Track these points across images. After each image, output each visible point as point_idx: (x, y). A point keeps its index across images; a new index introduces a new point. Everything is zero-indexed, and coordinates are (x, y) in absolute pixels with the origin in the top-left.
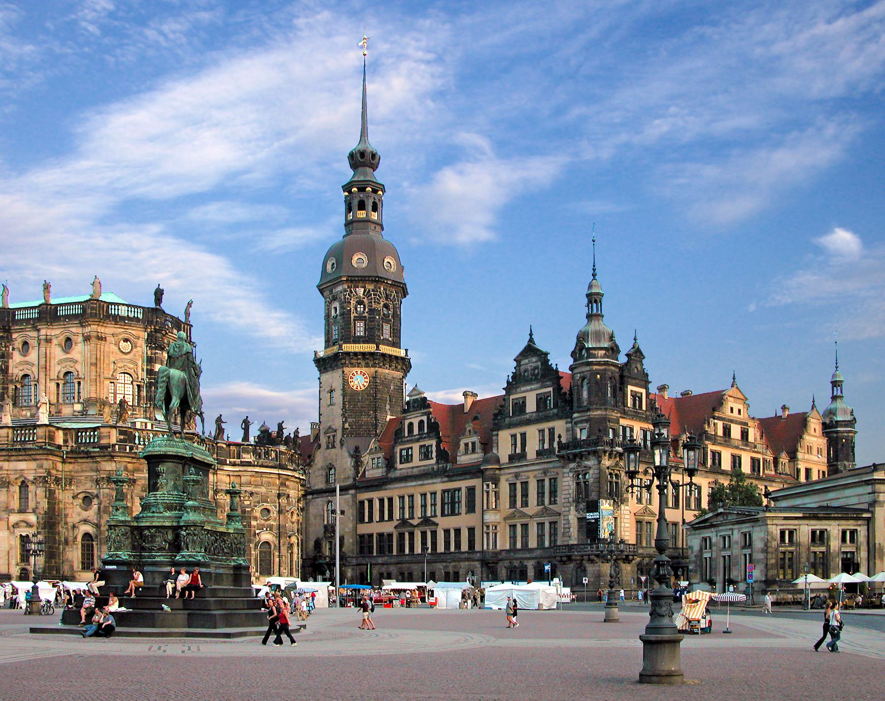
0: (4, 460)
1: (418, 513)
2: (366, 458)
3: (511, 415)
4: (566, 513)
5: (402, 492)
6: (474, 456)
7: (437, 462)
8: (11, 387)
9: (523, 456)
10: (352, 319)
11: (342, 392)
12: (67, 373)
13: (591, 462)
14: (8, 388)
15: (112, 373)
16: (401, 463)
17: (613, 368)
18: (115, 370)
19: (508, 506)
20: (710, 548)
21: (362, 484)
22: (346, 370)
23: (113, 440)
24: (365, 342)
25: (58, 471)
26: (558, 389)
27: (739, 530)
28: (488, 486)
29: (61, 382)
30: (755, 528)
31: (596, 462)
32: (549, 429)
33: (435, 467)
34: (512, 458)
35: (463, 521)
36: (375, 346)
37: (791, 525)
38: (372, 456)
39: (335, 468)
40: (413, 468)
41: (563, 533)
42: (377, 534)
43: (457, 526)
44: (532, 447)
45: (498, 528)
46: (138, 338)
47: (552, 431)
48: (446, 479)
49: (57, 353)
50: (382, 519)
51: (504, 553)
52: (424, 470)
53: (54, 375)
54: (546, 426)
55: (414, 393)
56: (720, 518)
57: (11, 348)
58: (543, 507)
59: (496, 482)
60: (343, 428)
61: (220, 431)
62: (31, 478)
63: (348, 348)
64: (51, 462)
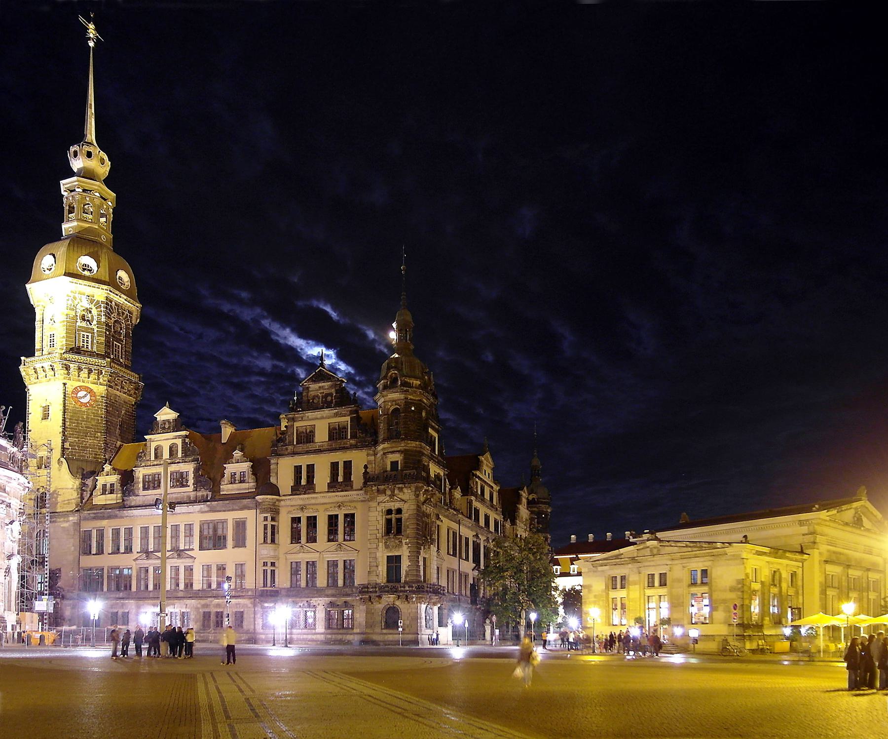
3: (295, 443)
4: (373, 551)
7: (195, 490)
9: (310, 486)
16: (144, 489)
19: (289, 541)
33: (192, 495)
34: (297, 489)
43: (220, 561)
44: (322, 478)
50: (116, 551)
52: (176, 498)
54: (340, 457)
59: (275, 512)
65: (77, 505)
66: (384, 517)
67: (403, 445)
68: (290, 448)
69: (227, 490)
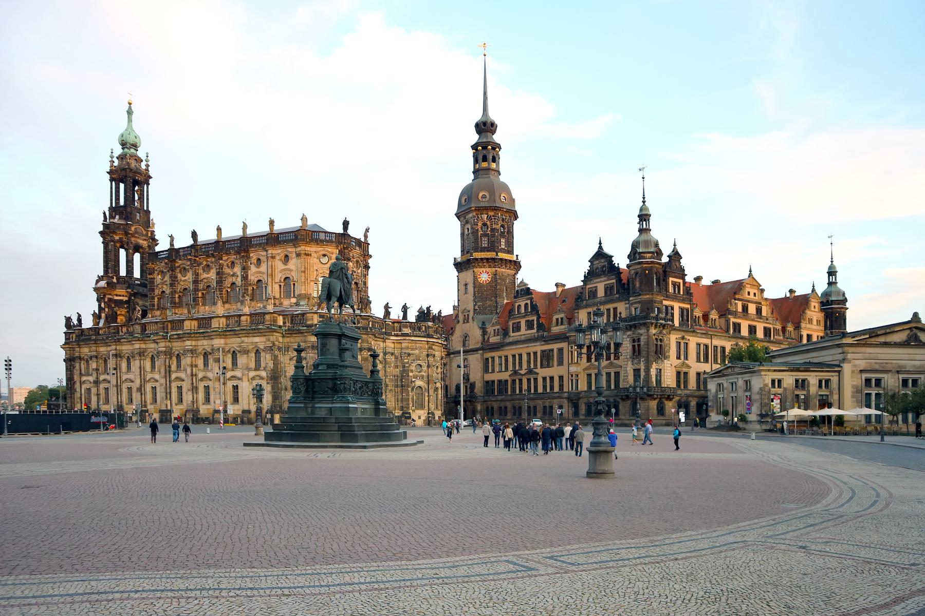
0: (245, 336)
1: (525, 366)
2: (490, 330)
4: (625, 366)
5: (516, 352)
6: (563, 327)
7: (538, 331)
8: (250, 288)
10: (479, 235)
12: (286, 278)
13: (642, 331)
14: (247, 289)
15: (315, 277)
17: (657, 266)
18: (317, 275)
20: (723, 391)
21: (487, 347)
22: (475, 269)
23: (315, 322)
24: (488, 251)
25: (279, 342)
26: (619, 280)
27: (742, 378)
28: (572, 347)
29: (282, 284)
30: (754, 378)
31: (646, 331)
33: (536, 335)
35: (555, 371)
37: (777, 376)
38: (494, 328)
40: (521, 335)
41: (624, 379)
43: (551, 375)
45: (579, 376)
46: (333, 254)
47: (615, 309)
48: (543, 343)
49: (279, 265)
51: (583, 393)
53: (277, 280)
54: (611, 306)
55: (522, 285)
56: (729, 370)
60: (475, 310)
61: (387, 313)
62: (262, 347)
64: (275, 337)
65: (482, 344)
68: (585, 302)
69: (555, 330)
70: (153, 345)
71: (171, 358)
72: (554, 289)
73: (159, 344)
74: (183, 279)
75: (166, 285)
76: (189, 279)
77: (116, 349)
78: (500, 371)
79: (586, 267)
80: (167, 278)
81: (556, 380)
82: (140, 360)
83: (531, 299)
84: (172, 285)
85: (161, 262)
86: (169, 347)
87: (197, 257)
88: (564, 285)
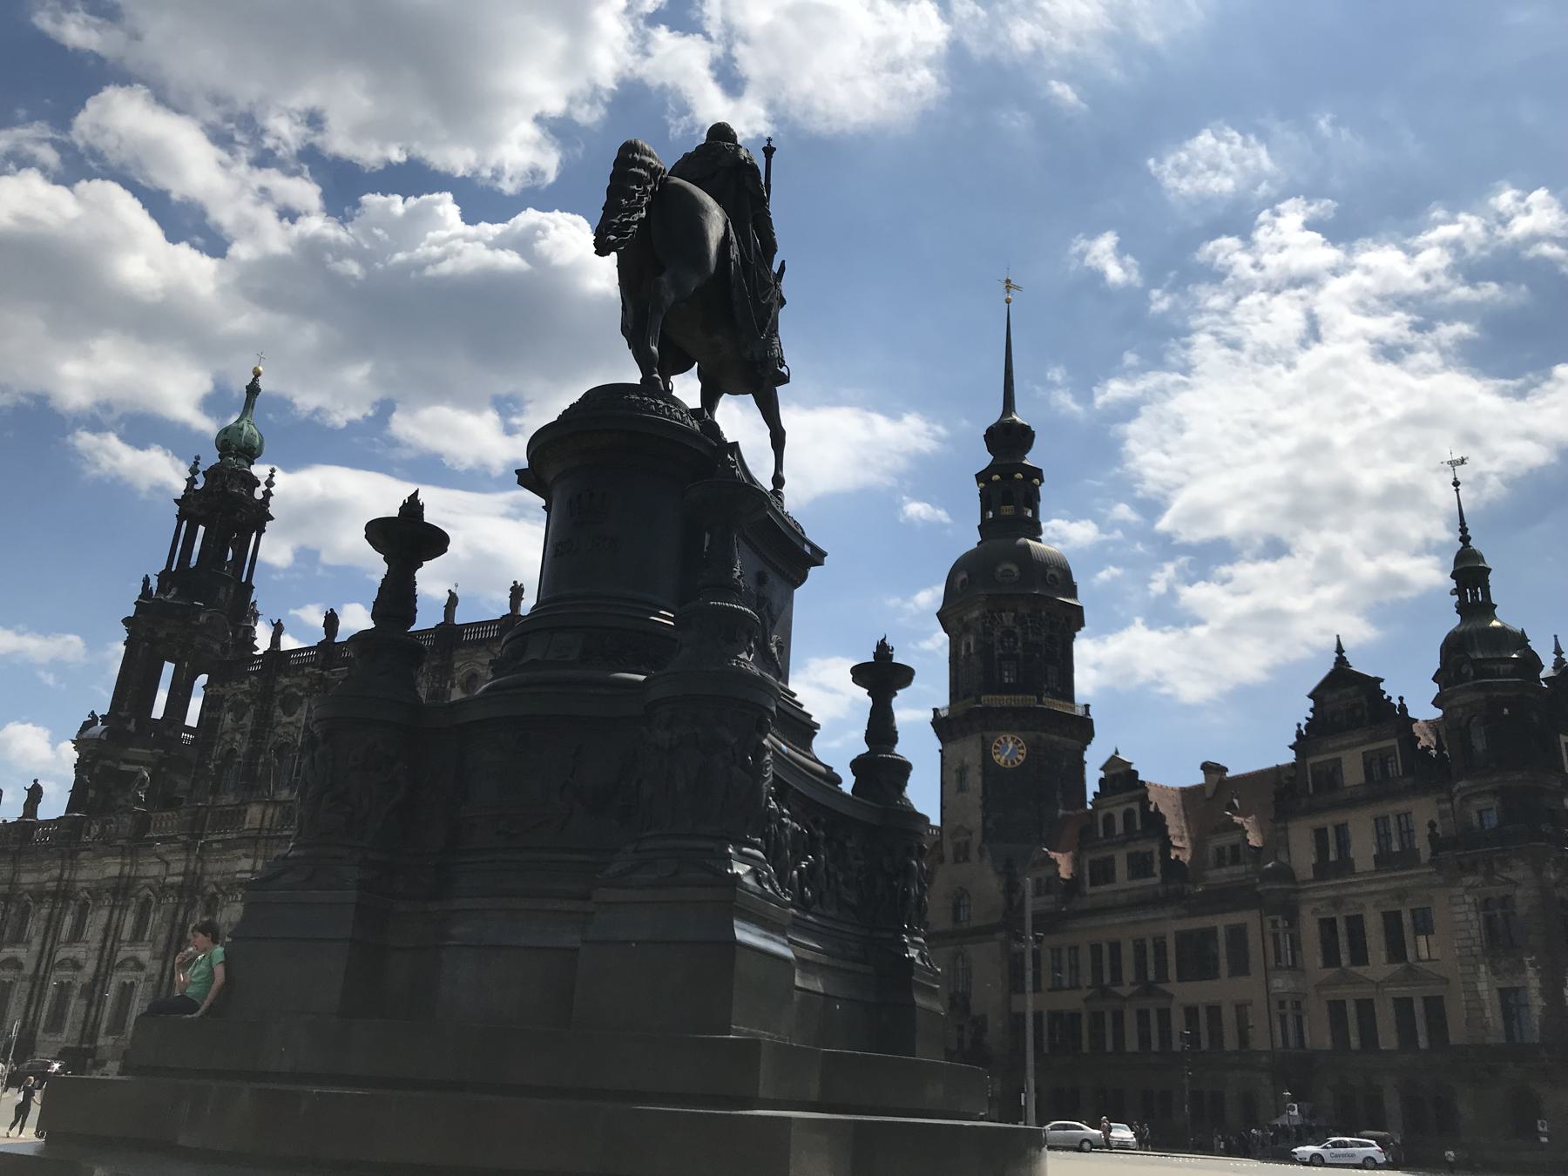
1: (1129, 973)
3: (1311, 791)
6: (1241, 869)
9: (1345, 865)
11: (980, 770)
16: (1093, 884)
19: (1319, 962)
22: (988, 735)
28: (1274, 923)
32: (1399, 816)
34: (1323, 870)
35: (1222, 990)
36: (1035, 697)
39: (969, 896)
42: (1049, 1011)
44: (1363, 849)
47: (1404, 818)
54: (1390, 809)
57: (449, 683)
58: (1403, 965)
59: (1292, 915)
63: (989, 700)
66: (1481, 913)
67: (1496, 779)
70: (155, 870)
71: (191, 906)
72: (1199, 778)
73: (172, 865)
74: (285, 719)
75: (242, 734)
76: (299, 720)
77: (60, 879)
78: (1057, 988)
79: (1303, 710)
80: (247, 721)
81: (1228, 1017)
82: (113, 907)
83: (1144, 800)
84: (257, 735)
85: (242, 683)
86: (195, 873)
87: (329, 669)
88: (1226, 770)
